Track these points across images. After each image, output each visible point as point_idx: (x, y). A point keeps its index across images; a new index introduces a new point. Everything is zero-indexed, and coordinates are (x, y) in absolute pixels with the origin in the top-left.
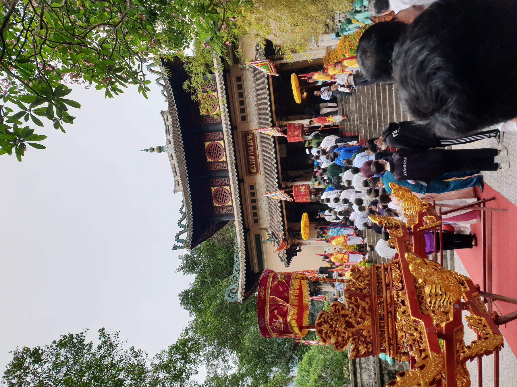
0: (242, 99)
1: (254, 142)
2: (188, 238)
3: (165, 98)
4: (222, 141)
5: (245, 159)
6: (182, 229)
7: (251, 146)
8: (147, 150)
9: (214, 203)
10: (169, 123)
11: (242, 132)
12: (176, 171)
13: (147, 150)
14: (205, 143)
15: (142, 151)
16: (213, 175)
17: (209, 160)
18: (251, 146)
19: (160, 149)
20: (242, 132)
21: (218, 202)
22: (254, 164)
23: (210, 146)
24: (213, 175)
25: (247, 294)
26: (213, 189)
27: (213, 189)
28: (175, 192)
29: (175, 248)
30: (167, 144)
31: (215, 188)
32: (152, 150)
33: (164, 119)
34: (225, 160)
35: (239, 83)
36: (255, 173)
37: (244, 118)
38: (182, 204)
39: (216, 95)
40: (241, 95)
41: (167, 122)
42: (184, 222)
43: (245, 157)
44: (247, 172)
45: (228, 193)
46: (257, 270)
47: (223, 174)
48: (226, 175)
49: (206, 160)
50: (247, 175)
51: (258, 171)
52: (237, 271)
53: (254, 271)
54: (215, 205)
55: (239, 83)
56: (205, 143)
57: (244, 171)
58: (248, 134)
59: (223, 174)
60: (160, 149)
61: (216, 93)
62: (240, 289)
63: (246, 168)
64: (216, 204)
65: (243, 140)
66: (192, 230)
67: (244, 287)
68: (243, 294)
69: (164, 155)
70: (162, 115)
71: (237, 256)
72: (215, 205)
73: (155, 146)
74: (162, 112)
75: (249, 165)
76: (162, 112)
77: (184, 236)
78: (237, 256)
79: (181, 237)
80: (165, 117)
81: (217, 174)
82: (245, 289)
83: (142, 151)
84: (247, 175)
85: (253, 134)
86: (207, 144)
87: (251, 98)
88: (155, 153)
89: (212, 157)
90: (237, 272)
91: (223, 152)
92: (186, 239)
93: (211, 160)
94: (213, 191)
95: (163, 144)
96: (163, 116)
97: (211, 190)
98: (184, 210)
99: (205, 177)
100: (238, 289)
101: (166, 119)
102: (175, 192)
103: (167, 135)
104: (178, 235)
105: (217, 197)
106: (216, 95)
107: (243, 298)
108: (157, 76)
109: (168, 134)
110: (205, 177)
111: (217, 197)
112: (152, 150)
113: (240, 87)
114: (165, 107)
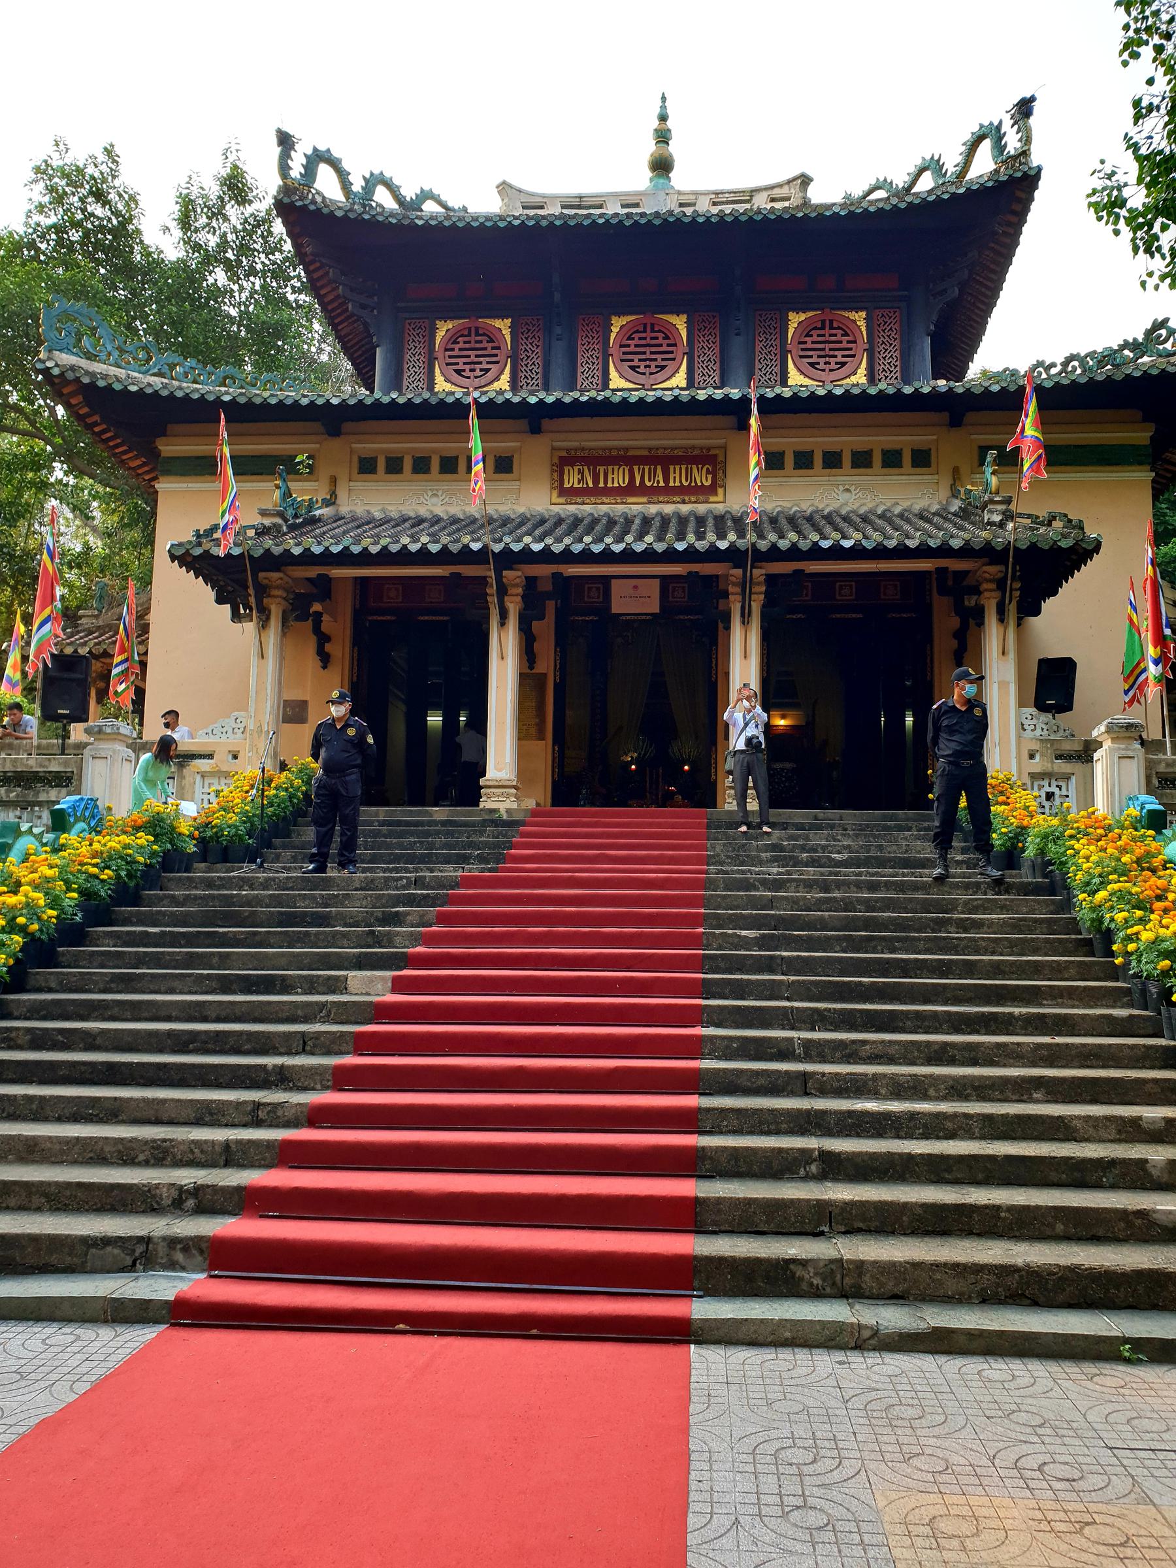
0: (847, 460)
1: (682, 490)
2: (319, 199)
3: (857, 192)
4: (684, 384)
5: (618, 449)
6: (357, 186)
7: (666, 480)
8: (663, 118)
9: (450, 325)
10: (761, 202)
11: (724, 448)
12: (579, 207)
13: (663, 118)
14: (684, 318)
15: (664, 99)
16: (558, 330)
17: (617, 324)
18: (666, 480)
19: (662, 166)
21: (453, 339)
22: (596, 480)
23: (669, 333)
24: (558, 330)
25: (72, 394)
26: (504, 326)
27: (504, 326)
28: (504, 188)
29: (285, 141)
30: (679, 193)
31: (507, 333)
32: (663, 137)
33: (780, 186)
35: (907, 458)
36: (562, 481)
38: (454, 203)
40: (862, 460)
41: (764, 195)
42: (382, 197)
43: (627, 449)
44: (568, 450)
45: (483, 381)
46: (168, 448)
47: (557, 373)
48: (552, 382)
49: (619, 314)
50: (553, 449)
51: (568, 494)
52: (172, 367)
53: (164, 434)
54: (439, 324)
55: (907, 458)
56: (684, 318)
57: (572, 442)
58: (714, 473)
59: (557, 373)
60: (662, 166)
62: (98, 367)
63: (583, 449)
64: (443, 329)
65: (693, 447)
66: (352, 216)
67: (101, 383)
68: (70, 376)
69: (639, 179)
70: (795, 179)
71: (233, 378)
72: (439, 324)
73: (674, 148)
74: (805, 181)
75: (595, 461)
76: (805, 181)
77: (327, 185)
78: (233, 378)
79: (324, 170)
80: (784, 191)
81: (559, 349)
82: (93, 385)
83: (664, 99)
84: (553, 449)
85: (712, 490)
86: (680, 323)
87: (847, 495)
88: (649, 147)
89: (629, 333)
90: (165, 369)
91: (642, 379)
92: (318, 193)
93: (615, 329)
94: (498, 323)
95: (682, 179)
96: (789, 182)
97: (502, 317)
98: (430, 207)
99: (557, 296)
100: (90, 357)
101: (777, 192)
102: (504, 188)
103: (717, 193)
104: (335, 164)
105: (473, 338)
107: (56, 371)
108: (951, 162)
109: (717, 197)
110: (557, 296)
111: (473, 338)
112: (663, 137)
113: (892, 460)
114: (827, 193)
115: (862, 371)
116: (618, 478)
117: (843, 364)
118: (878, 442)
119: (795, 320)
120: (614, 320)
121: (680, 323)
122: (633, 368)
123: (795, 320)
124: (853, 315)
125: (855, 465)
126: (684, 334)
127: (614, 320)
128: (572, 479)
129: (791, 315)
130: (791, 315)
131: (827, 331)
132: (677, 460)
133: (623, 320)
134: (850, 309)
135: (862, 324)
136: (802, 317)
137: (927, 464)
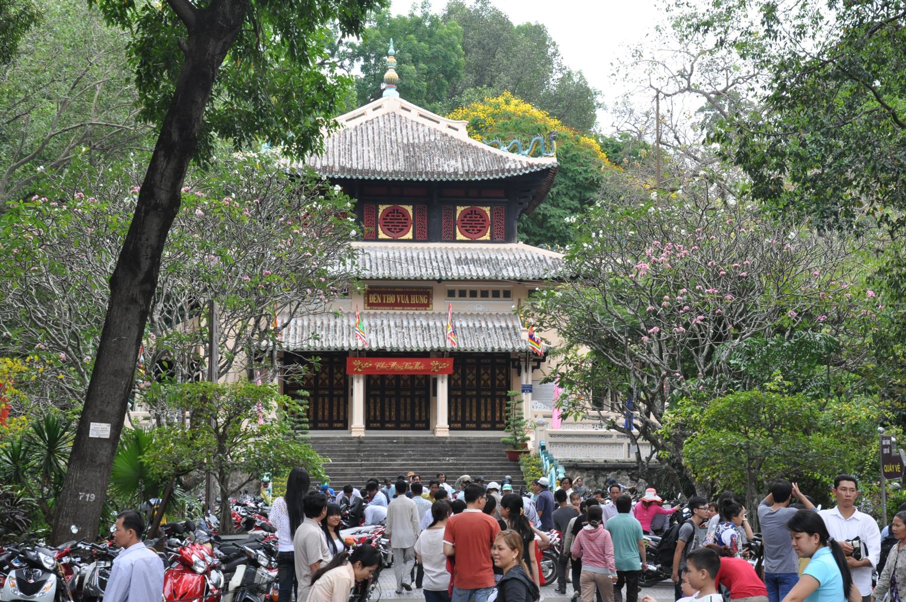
0: (479, 294)
4: (411, 237)
11: (432, 288)
14: (411, 207)
20: (432, 288)
34: (380, 237)
37: (451, 294)
39: (484, 238)
43: (394, 287)
49: (382, 204)
51: (371, 305)
56: (411, 207)
58: (428, 298)
61: (488, 238)
65: (420, 288)
85: (427, 306)
86: (409, 209)
89: (387, 213)
93: (381, 211)
106: (484, 238)
115: (488, 234)
116: (391, 299)
117: (480, 231)
118: (491, 287)
119: (460, 209)
120: (380, 206)
121: (409, 209)
122: (389, 229)
123: (460, 209)
124: (485, 209)
125: (482, 296)
126: (411, 214)
127: (380, 206)
128: (373, 299)
129: (458, 208)
130: (458, 208)
131: (473, 216)
132: (414, 293)
133: (385, 207)
134: (483, 206)
135: (488, 213)
136: (463, 208)
137: (509, 297)
